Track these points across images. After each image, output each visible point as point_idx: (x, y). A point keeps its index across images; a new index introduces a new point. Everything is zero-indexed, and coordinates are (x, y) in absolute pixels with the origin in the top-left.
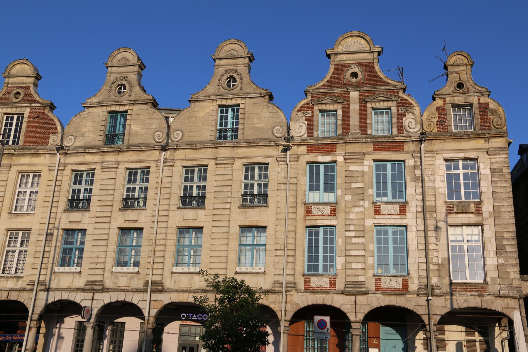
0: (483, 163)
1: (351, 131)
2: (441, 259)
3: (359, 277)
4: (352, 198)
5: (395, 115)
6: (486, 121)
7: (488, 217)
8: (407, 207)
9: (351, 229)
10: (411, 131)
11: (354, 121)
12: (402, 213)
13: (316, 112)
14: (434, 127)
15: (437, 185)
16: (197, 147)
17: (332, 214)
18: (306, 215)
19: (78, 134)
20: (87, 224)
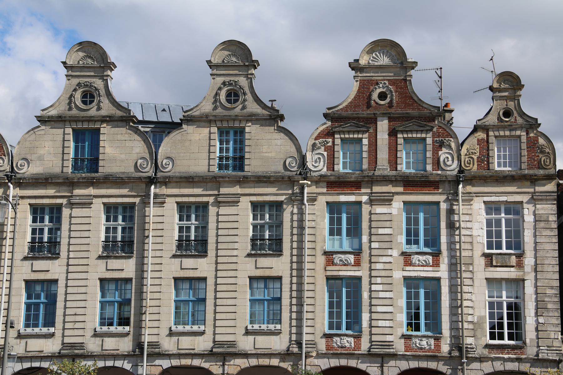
0: (528, 209)
1: (378, 166)
2: (477, 318)
3: (387, 336)
4: (379, 246)
5: (429, 148)
6: (533, 159)
7: (530, 271)
8: (441, 258)
9: (378, 282)
10: (448, 168)
11: (383, 155)
12: (435, 264)
13: (338, 141)
14: (473, 164)
15: (475, 233)
16: (195, 180)
17: (356, 264)
18: (327, 265)
19: (34, 157)
20: (57, 275)
